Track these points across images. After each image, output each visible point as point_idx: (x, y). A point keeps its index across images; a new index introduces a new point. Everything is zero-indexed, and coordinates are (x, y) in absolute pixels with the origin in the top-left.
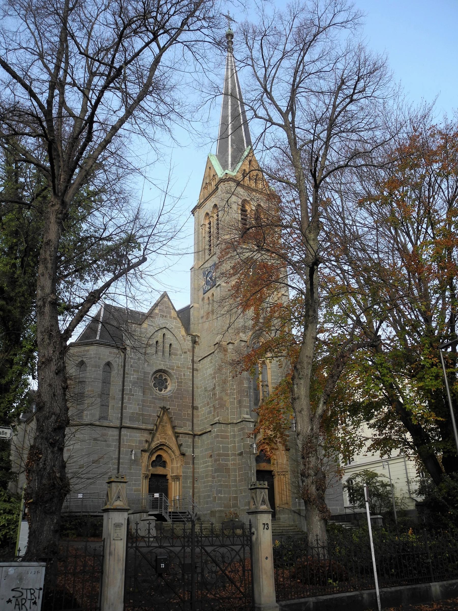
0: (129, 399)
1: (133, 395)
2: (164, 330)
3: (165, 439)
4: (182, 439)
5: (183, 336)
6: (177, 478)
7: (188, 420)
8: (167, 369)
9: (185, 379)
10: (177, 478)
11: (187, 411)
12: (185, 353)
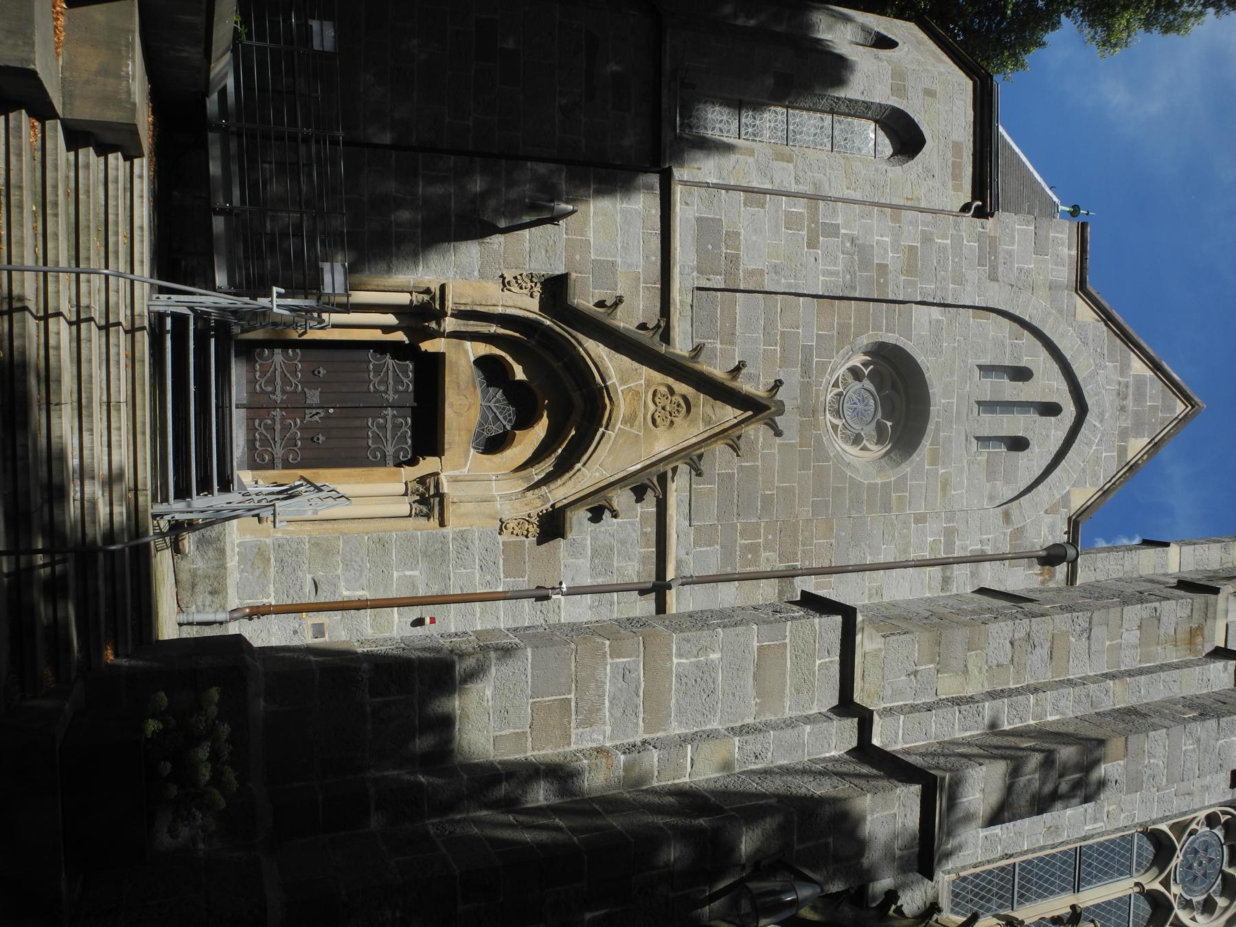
0: (792, 221)
1: (812, 244)
2: (1069, 410)
3: (630, 420)
4: (634, 518)
5: (1066, 499)
6: (429, 500)
7: (728, 551)
8: (931, 427)
9: (906, 524)
10: (429, 500)
11: (769, 547)
12: (1007, 517)
